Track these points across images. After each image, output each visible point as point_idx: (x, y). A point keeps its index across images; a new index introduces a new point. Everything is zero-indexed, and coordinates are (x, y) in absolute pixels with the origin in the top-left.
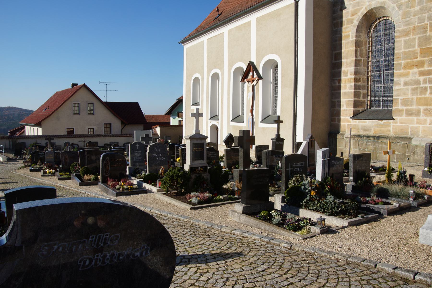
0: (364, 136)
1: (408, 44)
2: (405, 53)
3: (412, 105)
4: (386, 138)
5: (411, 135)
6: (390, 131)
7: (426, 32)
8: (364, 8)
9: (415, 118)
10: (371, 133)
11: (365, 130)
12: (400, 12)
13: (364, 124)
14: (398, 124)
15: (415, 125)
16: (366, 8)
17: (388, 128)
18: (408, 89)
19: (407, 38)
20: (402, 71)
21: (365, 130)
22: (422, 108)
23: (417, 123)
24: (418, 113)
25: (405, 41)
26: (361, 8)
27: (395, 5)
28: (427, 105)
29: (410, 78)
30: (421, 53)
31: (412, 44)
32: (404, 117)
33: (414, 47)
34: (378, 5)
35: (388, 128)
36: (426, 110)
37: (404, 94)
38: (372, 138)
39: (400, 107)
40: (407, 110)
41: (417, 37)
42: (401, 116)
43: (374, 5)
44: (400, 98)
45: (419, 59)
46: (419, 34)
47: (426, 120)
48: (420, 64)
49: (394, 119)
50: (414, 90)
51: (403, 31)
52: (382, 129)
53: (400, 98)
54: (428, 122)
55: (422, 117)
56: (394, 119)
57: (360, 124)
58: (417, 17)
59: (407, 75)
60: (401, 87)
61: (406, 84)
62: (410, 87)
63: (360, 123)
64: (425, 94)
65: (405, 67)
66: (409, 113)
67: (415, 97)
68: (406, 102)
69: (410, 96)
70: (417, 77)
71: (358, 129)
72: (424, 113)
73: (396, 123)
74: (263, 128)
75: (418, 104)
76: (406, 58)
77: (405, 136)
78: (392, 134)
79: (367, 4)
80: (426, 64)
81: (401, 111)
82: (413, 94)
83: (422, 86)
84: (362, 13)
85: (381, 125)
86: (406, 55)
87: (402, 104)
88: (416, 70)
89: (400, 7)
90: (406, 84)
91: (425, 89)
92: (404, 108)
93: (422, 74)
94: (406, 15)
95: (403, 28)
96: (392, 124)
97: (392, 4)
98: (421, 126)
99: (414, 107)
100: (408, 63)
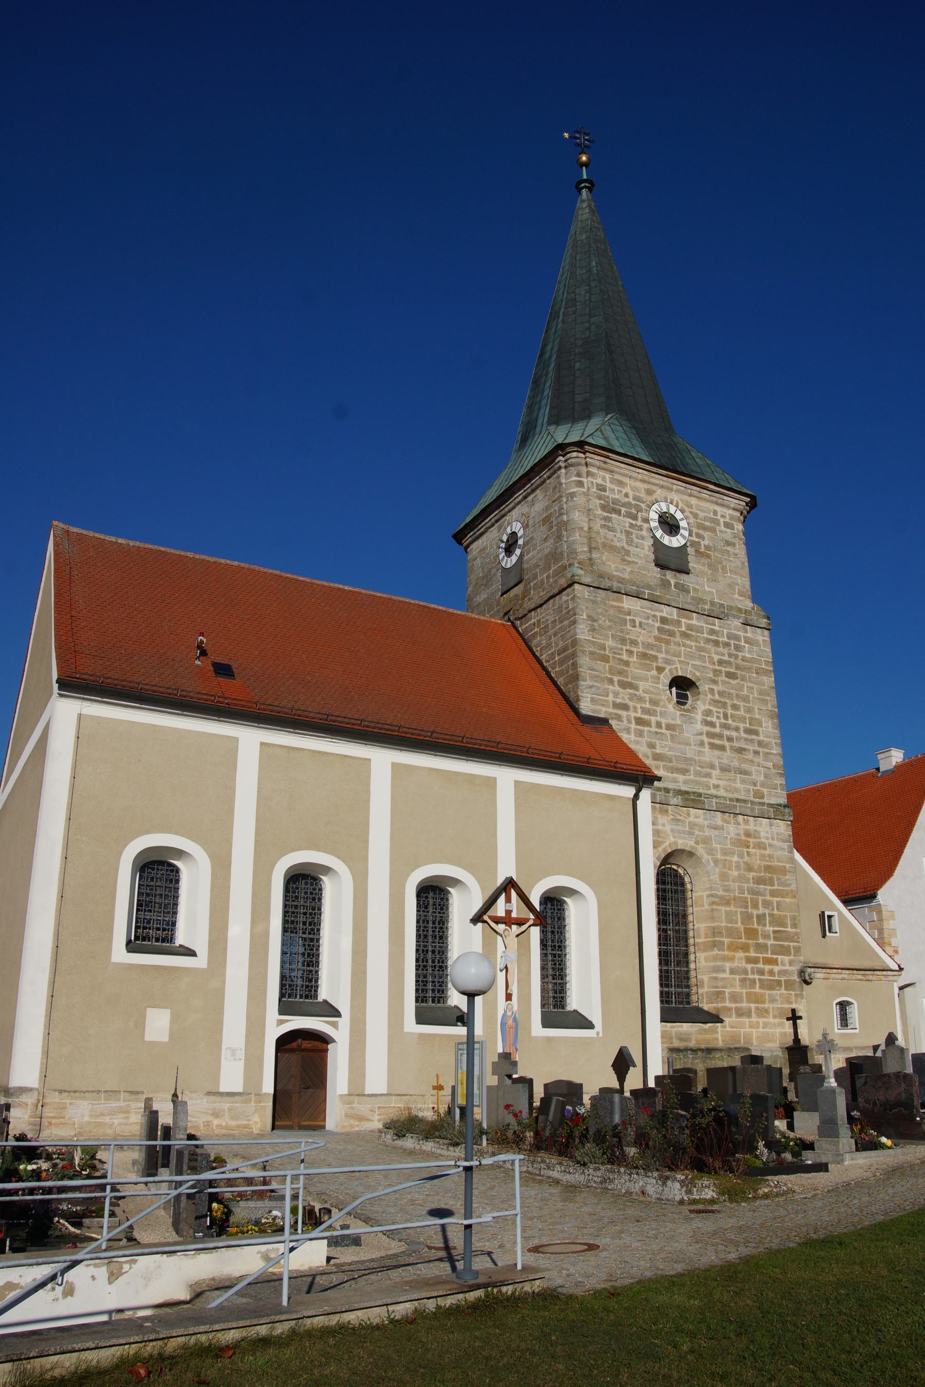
0: (686, 1050)
1: (730, 916)
2: (727, 929)
3: (742, 1001)
4: (721, 1050)
5: (744, 1043)
6: (717, 1039)
7: (747, 907)
8: (667, 843)
9: (747, 1020)
10: (692, 1044)
11: (681, 1040)
12: (717, 870)
13: (680, 1029)
14: (728, 1029)
15: (748, 1030)
16: (670, 845)
17: (716, 1036)
18: (735, 979)
19: (728, 909)
20: (726, 953)
21: (681, 1040)
22: (753, 1006)
23: (750, 1027)
24: (748, 1014)
25: (726, 911)
26: (664, 842)
27: (710, 857)
28: (757, 1002)
29: (736, 964)
30: (745, 933)
31: (734, 918)
32: (734, 1018)
33: (737, 923)
34: (687, 849)
35: (716, 1036)
36: (757, 1008)
37: (732, 986)
38: (699, 1052)
39: (728, 1004)
40: (736, 1008)
41: (739, 910)
42: (730, 1016)
43: (683, 843)
44: (727, 990)
45: (743, 940)
46: (741, 907)
47: (758, 1023)
48: (745, 948)
49: (721, 1021)
50: (743, 981)
51: (721, 897)
52: (708, 1036)
53: (727, 990)
54: (761, 1025)
55: (754, 1019)
56: (721, 1021)
57: (674, 1030)
58: (736, 884)
59: (732, 959)
60: (727, 975)
61: (732, 972)
62: (737, 977)
63: (674, 1027)
64: (755, 988)
65: (733, 947)
66: (740, 1013)
67: (744, 991)
68: (735, 998)
69: (738, 990)
70: (743, 964)
71: (671, 1038)
72: (756, 1013)
73: (725, 1027)
74: (549, 1039)
75: (749, 1001)
76: (729, 936)
77: (738, 1046)
78: (720, 1044)
79: (672, 839)
80: (752, 950)
81: (730, 1009)
82: (742, 987)
83: (750, 976)
84: (664, 850)
85: (705, 1030)
86: (731, 932)
87: (729, 999)
88: (740, 954)
89: (716, 862)
90: (732, 972)
91: (754, 980)
92: (733, 1005)
93: (749, 960)
94: (724, 876)
95: (721, 893)
96: (719, 1030)
97: (706, 856)
98: (754, 1030)
99: (744, 1005)
100: (732, 943)
